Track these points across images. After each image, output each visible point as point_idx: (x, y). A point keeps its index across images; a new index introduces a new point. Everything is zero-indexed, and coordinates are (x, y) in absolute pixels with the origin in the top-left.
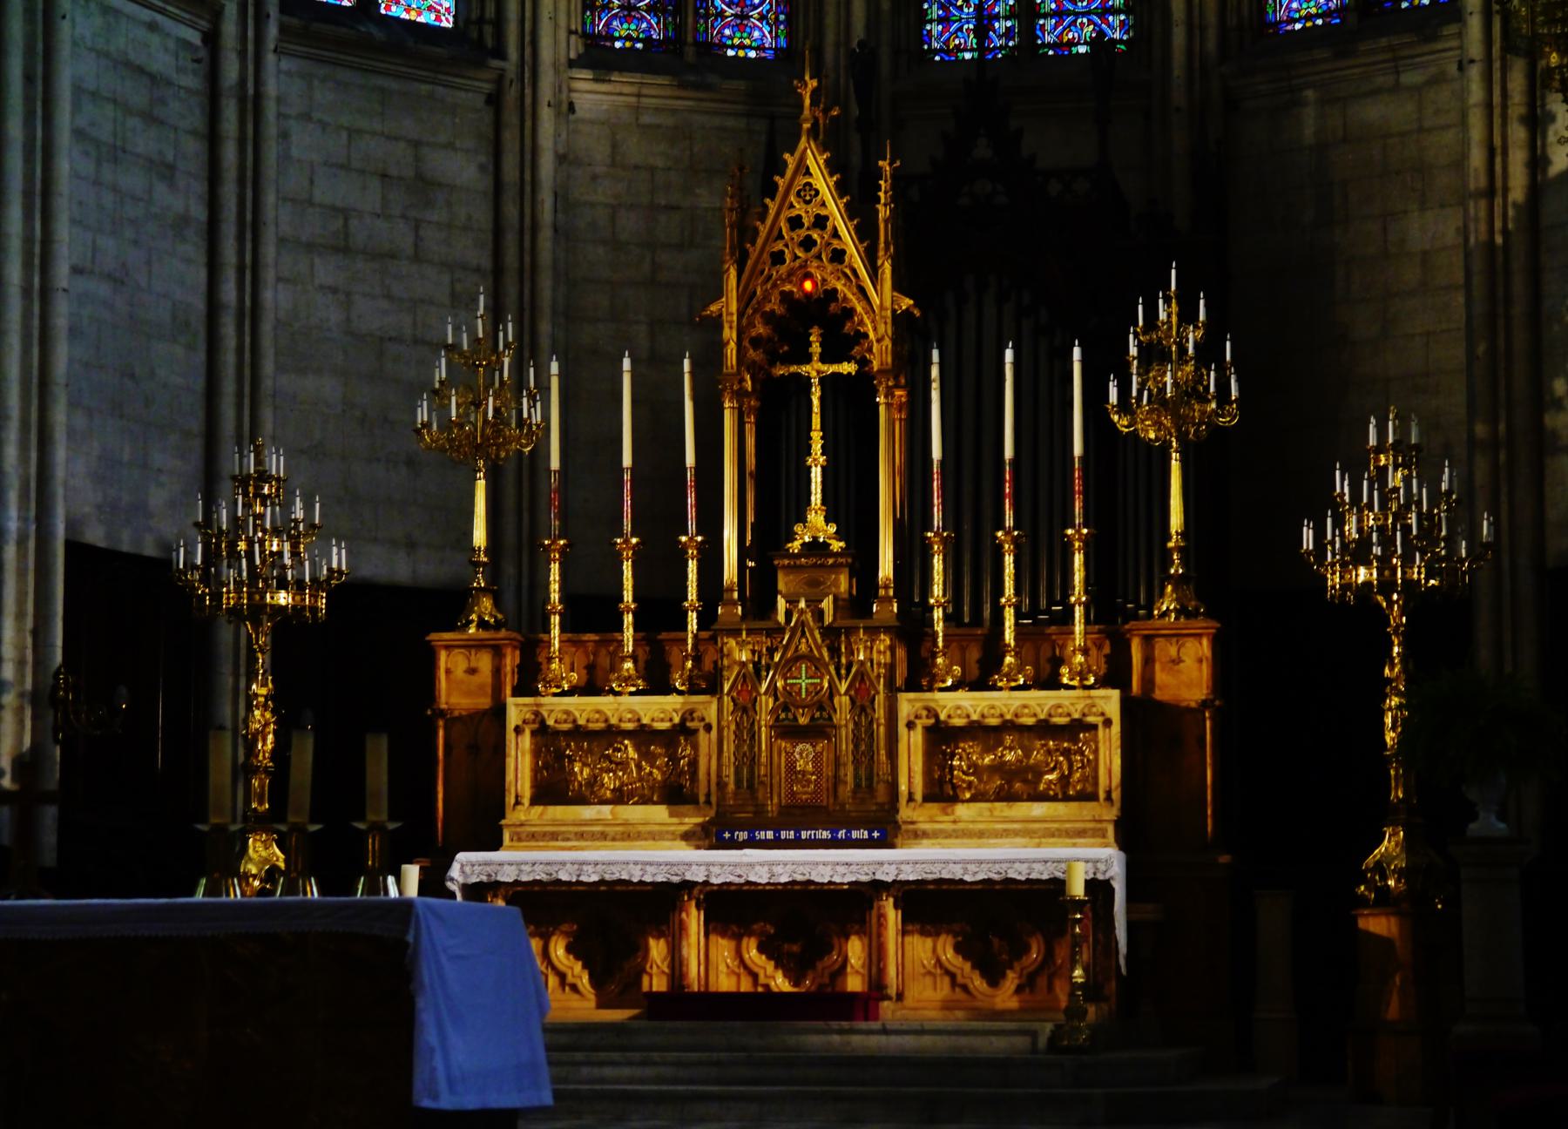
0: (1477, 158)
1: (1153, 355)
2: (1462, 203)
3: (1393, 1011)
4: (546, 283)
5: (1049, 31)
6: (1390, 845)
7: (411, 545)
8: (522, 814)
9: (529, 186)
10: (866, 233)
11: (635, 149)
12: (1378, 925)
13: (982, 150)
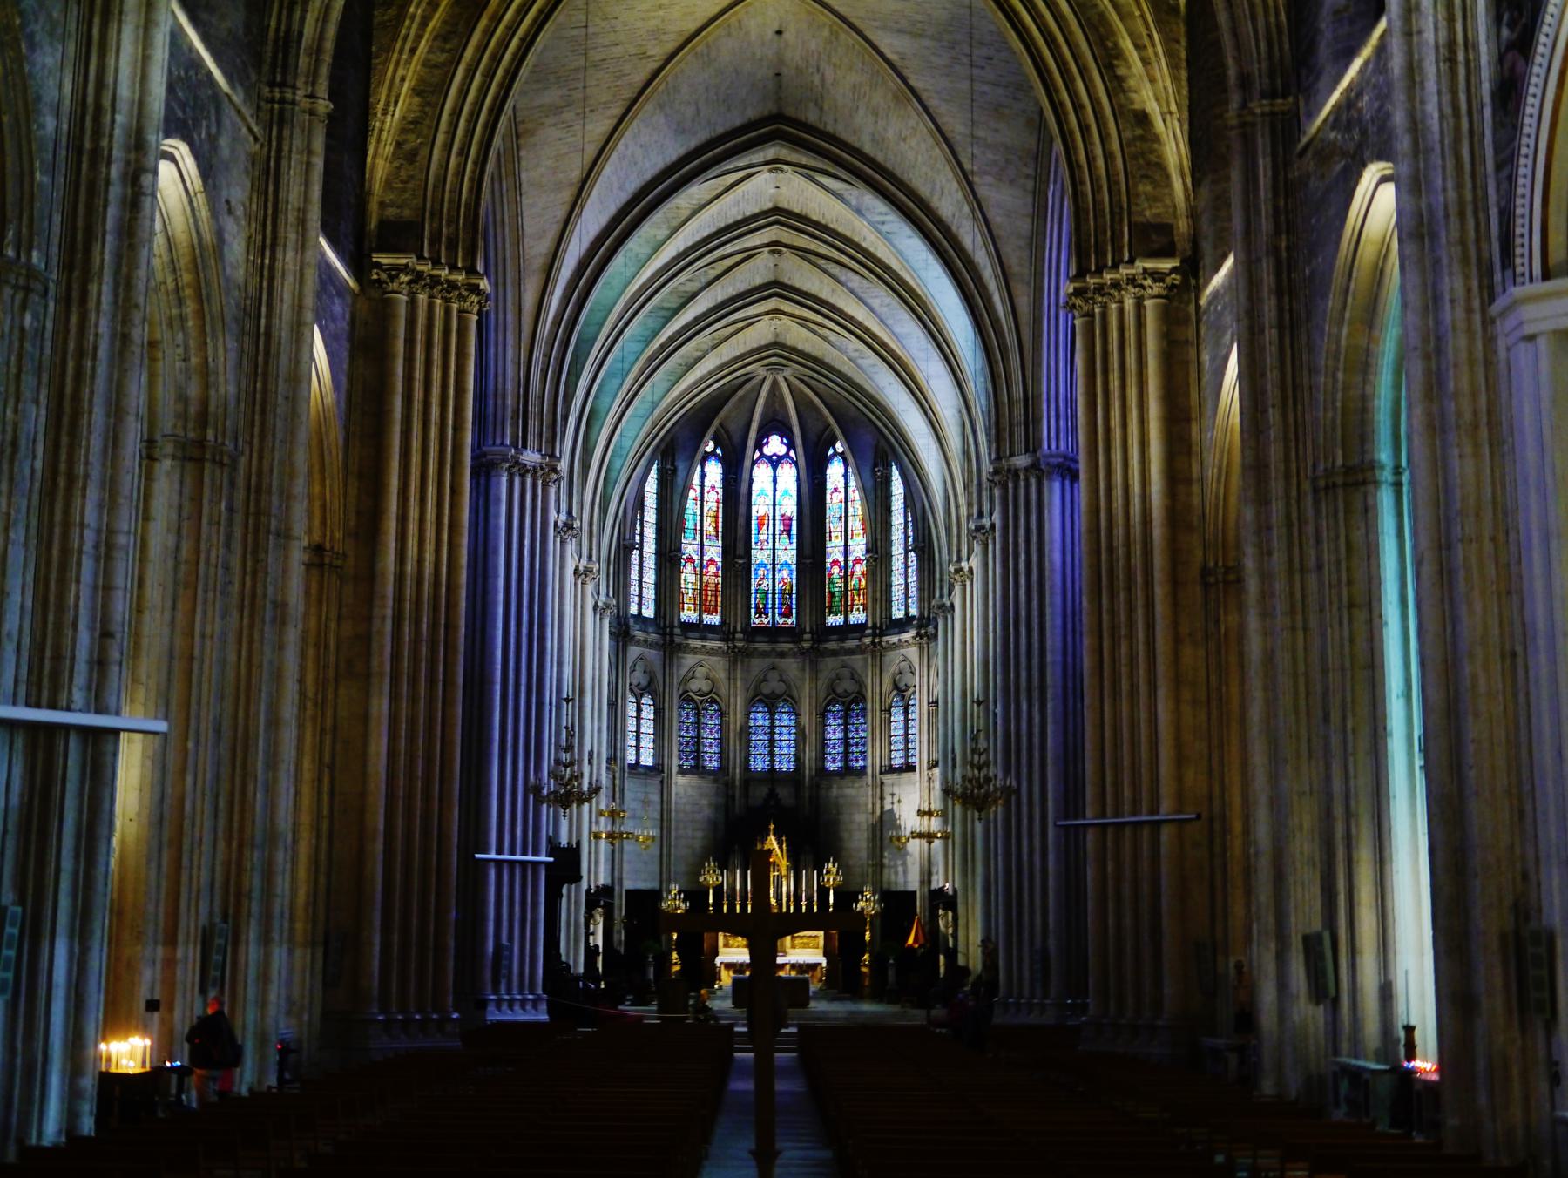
0: (870, 806)
1: (828, 872)
2: (866, 812)
3: (867, 983)
4: (673, 823)
5: (777, 766)
6: (866, 956)
7: (645, 880)
8: (721, 949)
9: (669, 802)
10: (782, 851)
11: (690, 791)
12: (864, 969)
13: (772, 803)
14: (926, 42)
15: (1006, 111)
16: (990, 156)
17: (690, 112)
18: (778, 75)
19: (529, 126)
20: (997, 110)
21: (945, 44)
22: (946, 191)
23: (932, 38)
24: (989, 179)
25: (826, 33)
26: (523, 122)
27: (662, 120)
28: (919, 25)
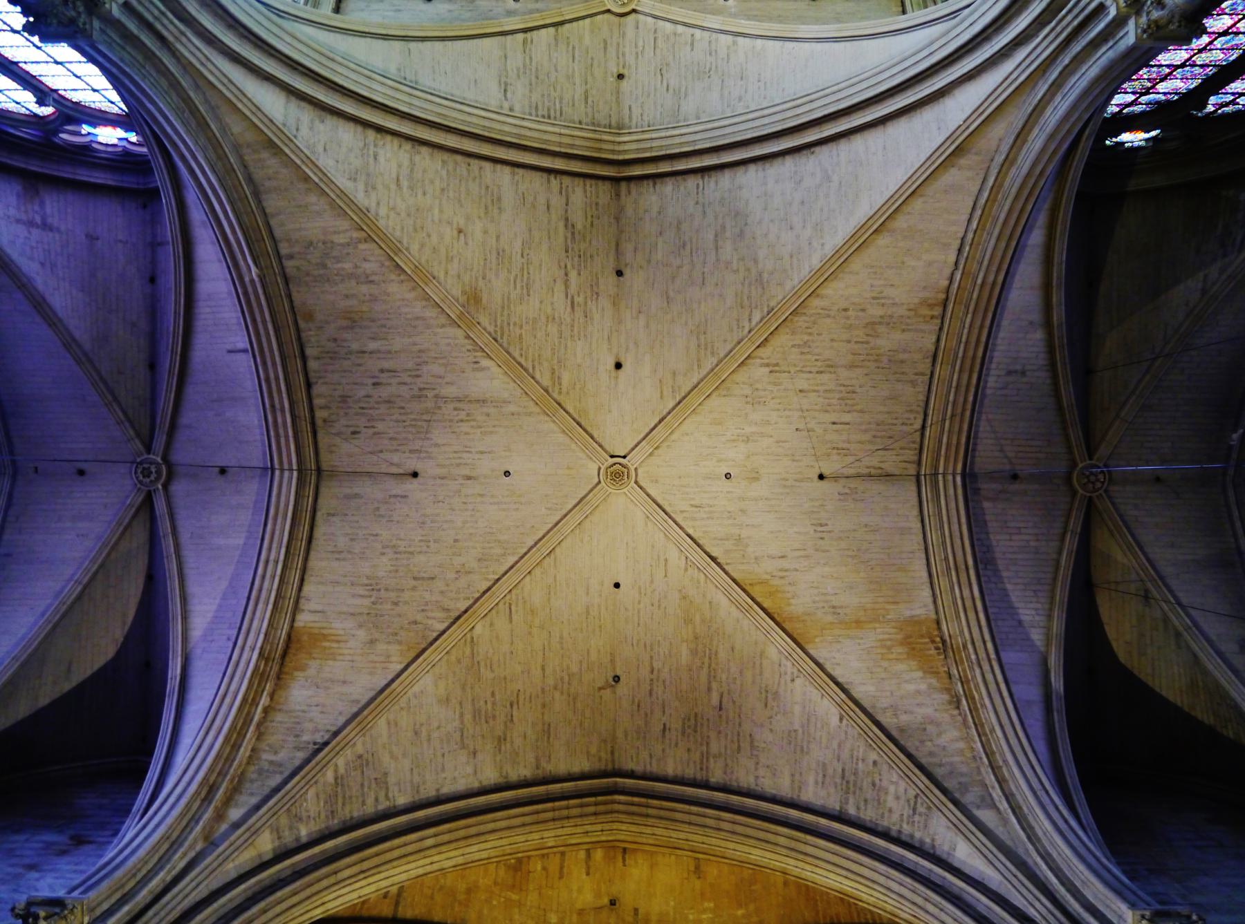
14: (450, 391)
15: (345, 323)
16: (347, 266)
17: (727, 249)
18: (619, 273)
19: (926, 312)
20: (352, 321)
21: (430, 394)
22: (393, 187)
23: (446, 399)
24: (340, 239)
25: (566, 378)
26: (932, 317)
27: (761, 254)
28: (463, 415)
